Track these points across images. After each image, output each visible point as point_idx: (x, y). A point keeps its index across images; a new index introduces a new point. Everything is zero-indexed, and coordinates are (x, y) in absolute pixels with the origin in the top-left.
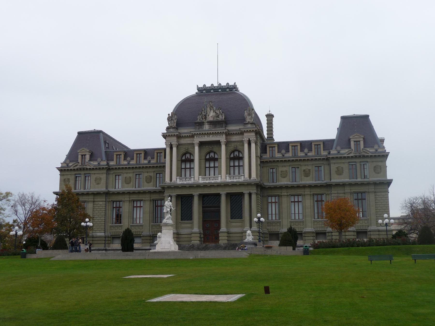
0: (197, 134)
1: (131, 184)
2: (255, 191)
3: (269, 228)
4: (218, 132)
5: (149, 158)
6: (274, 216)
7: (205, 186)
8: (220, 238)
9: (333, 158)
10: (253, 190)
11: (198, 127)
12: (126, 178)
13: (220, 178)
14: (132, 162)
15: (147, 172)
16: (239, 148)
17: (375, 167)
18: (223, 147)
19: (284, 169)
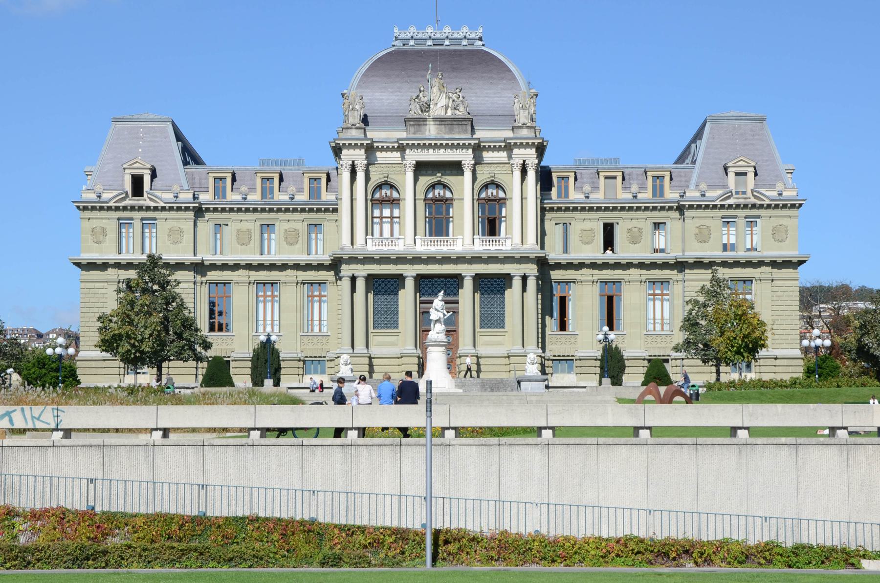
1: (252, 245)
4: (458, 144)
9: (691, 207)
10: (532, 270)
11: (412, 129)
12: (238, 231)
13: (459, 242)
17: (775, 229)
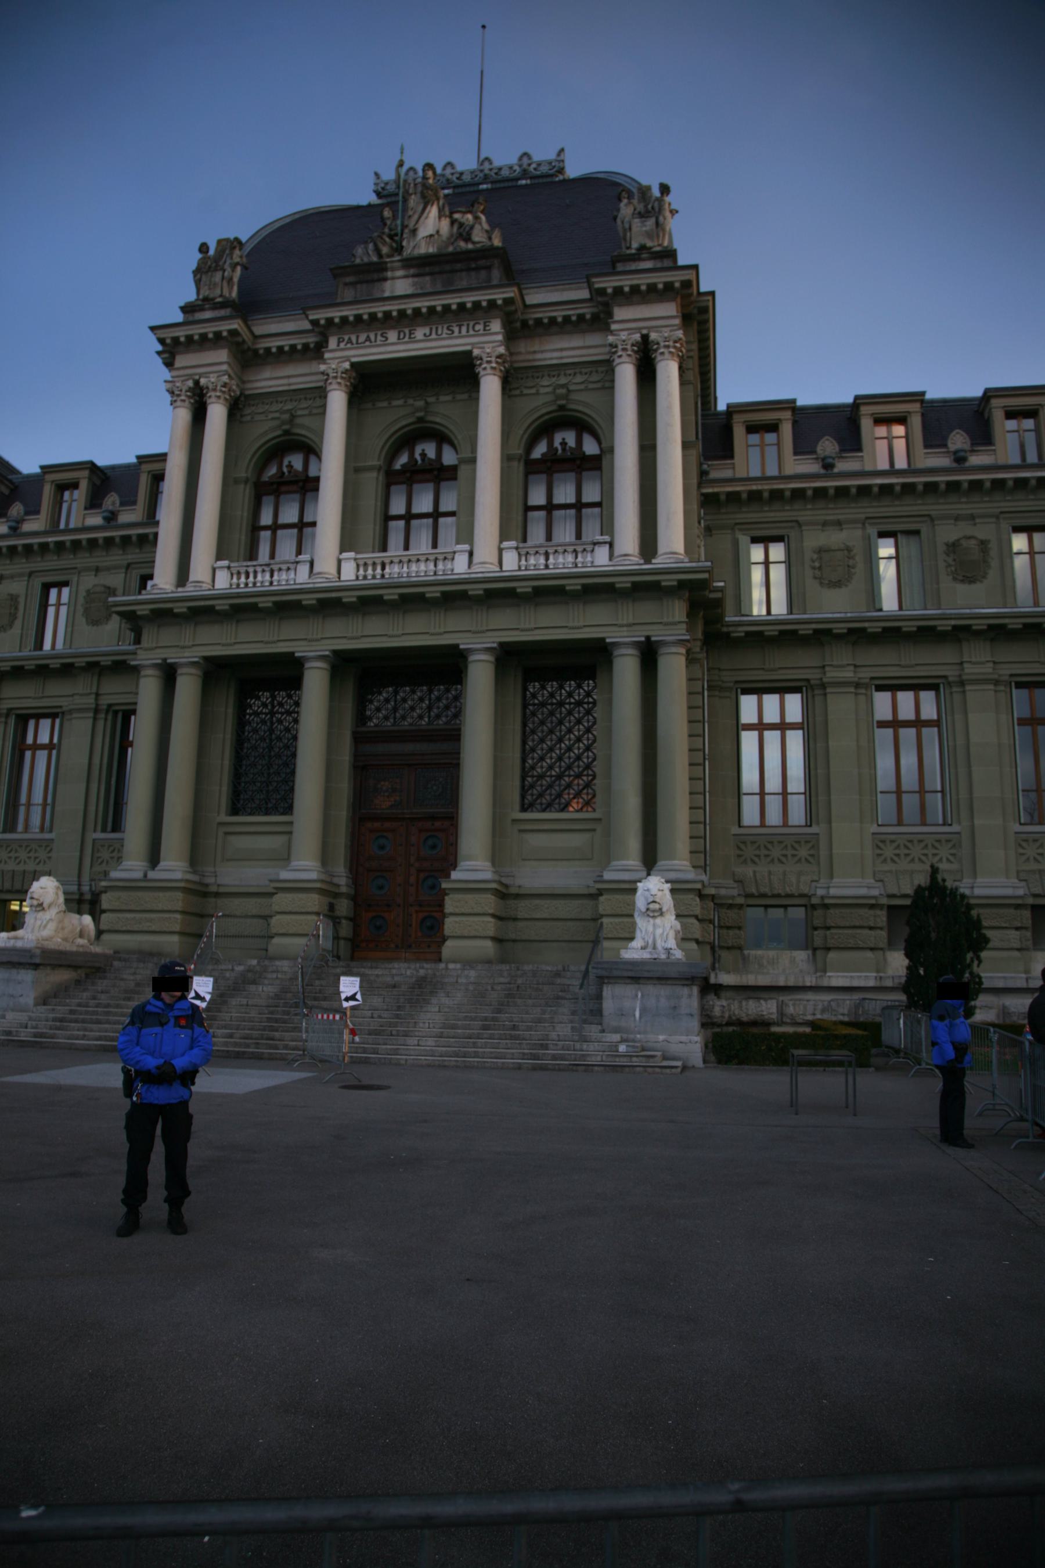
0: (344, 320)
2: (681, 632)
3: (748, 871)
5: (111, 501)
6: (774, 805)
7: (368, 603)
8: (450, 925)
10: (671, 623)
14: (31, 525)
15: (97, 570)
16: (584, 402)
18: (490, 387)
19: (835, 538)
